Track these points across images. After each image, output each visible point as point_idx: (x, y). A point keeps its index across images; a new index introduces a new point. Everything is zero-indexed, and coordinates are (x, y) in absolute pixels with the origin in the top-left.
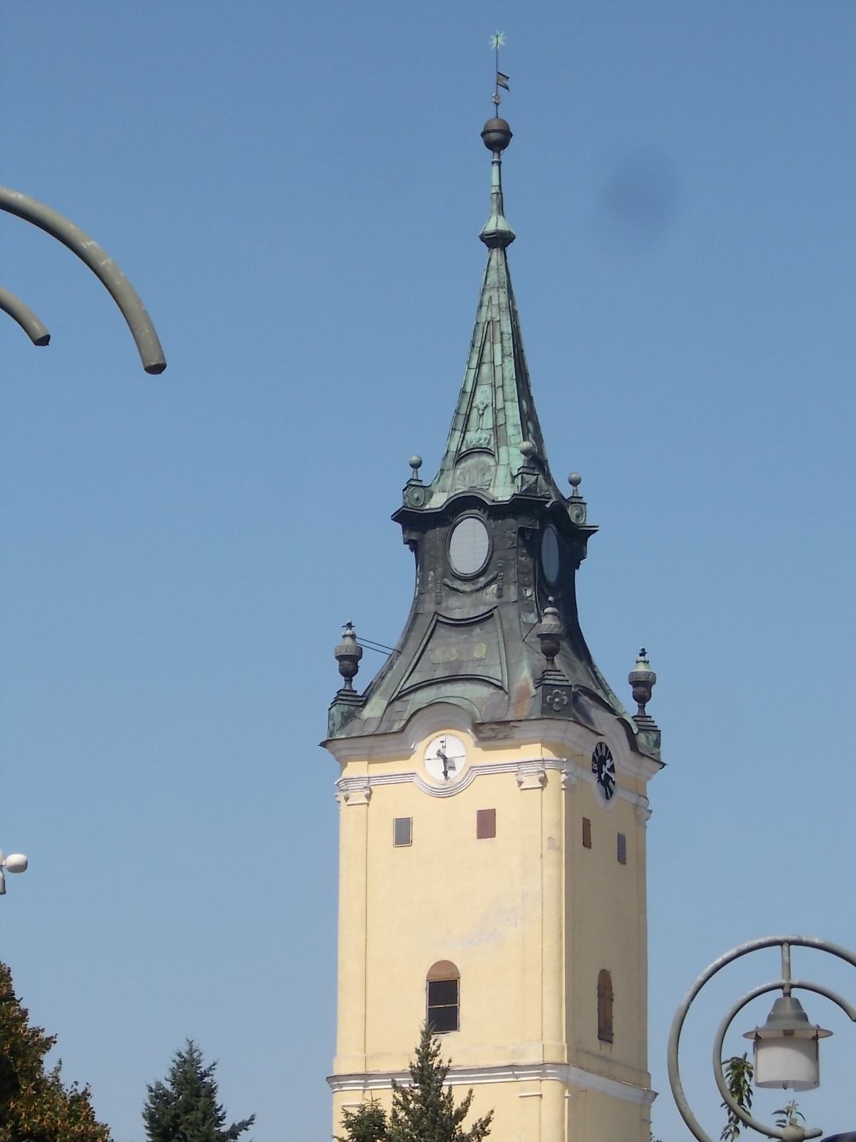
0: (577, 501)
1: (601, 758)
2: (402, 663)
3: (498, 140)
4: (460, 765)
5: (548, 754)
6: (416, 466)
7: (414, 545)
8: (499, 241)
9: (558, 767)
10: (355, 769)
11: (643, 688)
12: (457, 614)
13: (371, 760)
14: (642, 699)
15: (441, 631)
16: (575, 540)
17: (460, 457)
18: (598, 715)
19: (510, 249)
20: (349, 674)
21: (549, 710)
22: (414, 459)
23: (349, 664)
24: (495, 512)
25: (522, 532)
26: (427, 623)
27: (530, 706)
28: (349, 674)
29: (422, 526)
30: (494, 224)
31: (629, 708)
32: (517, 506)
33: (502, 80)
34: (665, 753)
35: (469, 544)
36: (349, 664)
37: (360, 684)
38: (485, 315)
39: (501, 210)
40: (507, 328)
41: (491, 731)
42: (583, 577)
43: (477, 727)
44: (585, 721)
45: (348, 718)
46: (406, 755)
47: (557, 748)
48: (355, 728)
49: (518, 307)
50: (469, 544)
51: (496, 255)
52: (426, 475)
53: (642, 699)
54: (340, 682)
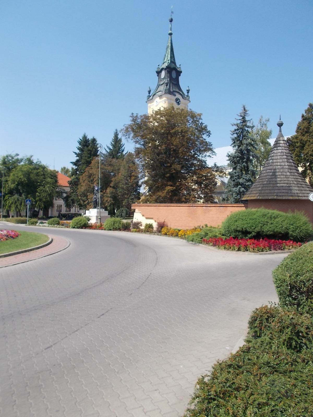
0: (180, 68)
1: (177, 100)
2: (155, 91)
3: (171, 21)
4: (158, 102)
5: (166, 99)
6: (159, 65)
7: (158, 76)
8: (171, 34)
9: (167, 100)
10: (149, 105)
11: (188, 91)
12: (161, 84)
13: (150, 103)
14: (188, 93)
15: (160, 86)
16: (179, 73)
17: (164, 63)
18: (177, 94)
19: (172, 35)
20: (149, 93)
21: (165, 93)
22: (158, 65)
23: (149, 92)
24: (165, 69)
25: (167, 71)
26: (158, 86)
27: (164, 93)
28: (149, 93)
29: (159, 73)
30: (170, 32)
31: (186, 94)
32: (168, 67)
33: (172, 12)
34: (190, 99)
35: (163, 74)
36: (149, 92)
37: (150, 95)
38: (168, 44)
39: (171, 30)
40: (170, 45)
41: (160, 97)
42: (180, 78)
43: (159, 96)
44: (175, 95)
45: (148, 99)
46: (153, 102)
47: (167, 98)
48: (149, 99)
49: (173, 43)
50: (163, 74)
51: (170, 36)
52: (160, 67)
53: (188, 93)
54: (148, 94)
